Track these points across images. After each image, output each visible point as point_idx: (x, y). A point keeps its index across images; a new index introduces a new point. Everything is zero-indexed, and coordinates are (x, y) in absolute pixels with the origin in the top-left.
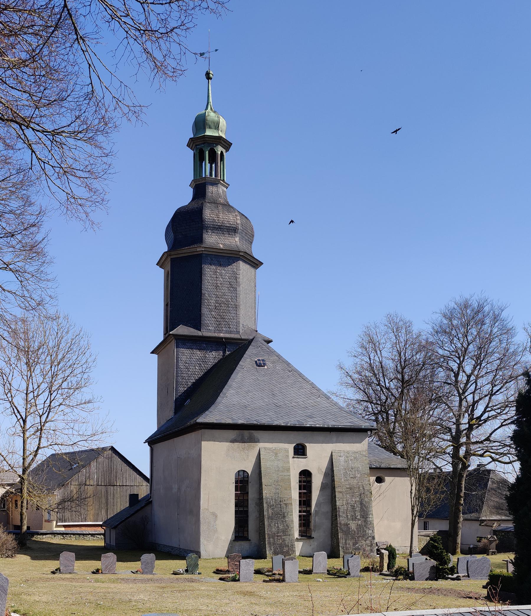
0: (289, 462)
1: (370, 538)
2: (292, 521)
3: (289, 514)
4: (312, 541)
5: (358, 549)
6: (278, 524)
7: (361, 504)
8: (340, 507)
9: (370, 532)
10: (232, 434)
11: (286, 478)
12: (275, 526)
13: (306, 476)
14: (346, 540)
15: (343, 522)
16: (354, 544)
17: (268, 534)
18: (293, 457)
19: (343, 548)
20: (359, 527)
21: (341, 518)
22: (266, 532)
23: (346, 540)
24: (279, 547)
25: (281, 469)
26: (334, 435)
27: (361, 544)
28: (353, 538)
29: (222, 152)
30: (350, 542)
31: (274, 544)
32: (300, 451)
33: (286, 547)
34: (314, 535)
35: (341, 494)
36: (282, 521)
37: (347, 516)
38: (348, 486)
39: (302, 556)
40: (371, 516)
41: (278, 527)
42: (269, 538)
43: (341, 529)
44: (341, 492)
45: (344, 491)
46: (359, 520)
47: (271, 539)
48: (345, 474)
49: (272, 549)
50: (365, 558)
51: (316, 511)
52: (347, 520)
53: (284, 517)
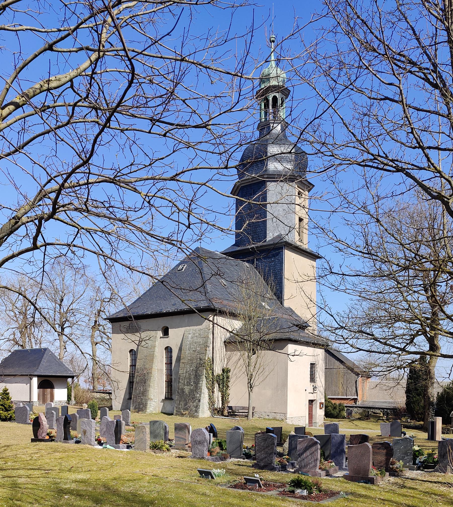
0: (155, 341)
1: (197, 401)
4: (172, 401)
7: (196, 372)
9: (198, 395)
10: (126, 324)
11: (152, 353)
13: (168, 350)
15: (180, 387)
16: (186, 404)
18: (161, 338)
19: (177, 407)
20: (191, 391)
21: (180, 384)
25: (150, 347)
26: (186, 318)
27: (189, 405)
28: (185, 400)
29: (275, 99)
32: (166, 332)
34: (173, 397)
35: (183, 365)
36: (144, 386)
37: (184, 382)
38: (189, 358)
39: (165, 413)
43: (178, 392)
44: (183, 363)
45: (186, 362)
46: (192, 385)
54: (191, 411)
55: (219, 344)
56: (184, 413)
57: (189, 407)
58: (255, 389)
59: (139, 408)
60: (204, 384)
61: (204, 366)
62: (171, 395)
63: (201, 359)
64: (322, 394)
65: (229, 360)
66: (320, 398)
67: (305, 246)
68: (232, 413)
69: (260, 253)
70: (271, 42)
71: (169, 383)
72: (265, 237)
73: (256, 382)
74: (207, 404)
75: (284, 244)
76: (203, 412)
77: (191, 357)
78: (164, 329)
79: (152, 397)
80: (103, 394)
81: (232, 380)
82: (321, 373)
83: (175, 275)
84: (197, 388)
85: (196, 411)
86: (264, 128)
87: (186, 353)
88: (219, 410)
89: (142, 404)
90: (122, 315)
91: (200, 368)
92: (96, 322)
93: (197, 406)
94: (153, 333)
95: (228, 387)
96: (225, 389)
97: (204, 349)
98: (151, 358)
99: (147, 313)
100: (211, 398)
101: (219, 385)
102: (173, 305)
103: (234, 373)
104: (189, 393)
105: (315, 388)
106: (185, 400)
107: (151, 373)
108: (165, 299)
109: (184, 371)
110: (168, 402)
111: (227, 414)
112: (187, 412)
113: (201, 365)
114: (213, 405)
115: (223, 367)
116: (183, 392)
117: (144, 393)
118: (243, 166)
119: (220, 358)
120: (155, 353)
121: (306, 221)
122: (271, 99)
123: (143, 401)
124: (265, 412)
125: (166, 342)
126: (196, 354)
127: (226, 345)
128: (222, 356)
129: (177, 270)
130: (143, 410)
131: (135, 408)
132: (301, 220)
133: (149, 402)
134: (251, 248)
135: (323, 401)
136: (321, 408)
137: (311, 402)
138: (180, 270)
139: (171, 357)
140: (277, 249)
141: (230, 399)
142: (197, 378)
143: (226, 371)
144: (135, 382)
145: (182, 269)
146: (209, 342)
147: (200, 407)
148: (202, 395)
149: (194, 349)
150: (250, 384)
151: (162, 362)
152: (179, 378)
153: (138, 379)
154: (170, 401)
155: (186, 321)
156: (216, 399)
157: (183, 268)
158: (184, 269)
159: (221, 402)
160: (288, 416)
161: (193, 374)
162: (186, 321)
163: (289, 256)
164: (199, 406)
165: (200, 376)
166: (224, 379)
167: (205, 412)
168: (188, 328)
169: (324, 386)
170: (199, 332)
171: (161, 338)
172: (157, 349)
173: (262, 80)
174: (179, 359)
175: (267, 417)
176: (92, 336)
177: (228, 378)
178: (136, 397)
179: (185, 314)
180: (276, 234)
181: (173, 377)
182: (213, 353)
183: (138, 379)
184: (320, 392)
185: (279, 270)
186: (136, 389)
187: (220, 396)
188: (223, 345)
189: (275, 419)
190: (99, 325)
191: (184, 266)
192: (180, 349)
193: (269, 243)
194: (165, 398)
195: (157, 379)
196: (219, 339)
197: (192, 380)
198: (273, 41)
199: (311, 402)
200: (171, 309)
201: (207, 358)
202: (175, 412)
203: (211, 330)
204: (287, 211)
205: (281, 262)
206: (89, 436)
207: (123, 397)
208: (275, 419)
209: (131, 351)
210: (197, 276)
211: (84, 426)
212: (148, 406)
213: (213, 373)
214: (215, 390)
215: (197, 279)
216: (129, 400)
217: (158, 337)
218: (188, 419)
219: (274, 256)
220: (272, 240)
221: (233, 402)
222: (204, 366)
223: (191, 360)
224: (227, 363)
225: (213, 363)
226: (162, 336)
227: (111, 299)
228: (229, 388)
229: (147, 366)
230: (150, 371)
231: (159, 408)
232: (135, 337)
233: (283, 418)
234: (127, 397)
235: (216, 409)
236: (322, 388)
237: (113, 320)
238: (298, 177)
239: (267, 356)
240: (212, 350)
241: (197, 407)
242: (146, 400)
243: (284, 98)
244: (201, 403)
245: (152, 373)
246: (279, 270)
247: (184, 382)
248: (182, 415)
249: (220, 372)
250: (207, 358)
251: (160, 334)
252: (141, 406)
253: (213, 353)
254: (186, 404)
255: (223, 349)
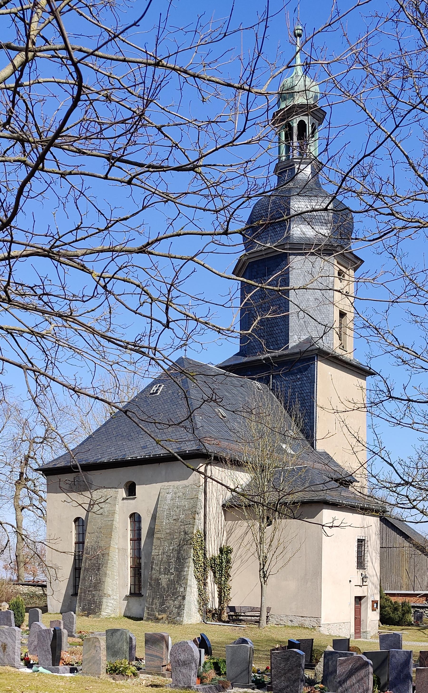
1: (180, 598)
2: (106, 574)
3: (104, 566)
4: (142, 598)
5: (163, 611)
6: (92, 577)
7: (179, 553)
8: (155, 557)
9: (182, 589)
10: (70, 477)
11: (110, 523)
12: (89, 579)
14: (153, 599)
16: (162, 603)
17: (81, 588)
18: (123, 499)
19: (148, 608)
20: (171, 583)
22: (80, 586)
23: (153, 599)
24: (88, 603)
27: (168, 604)
28: (161, 597)
29: (302, 125)
30: (157, 602)
31: (84, 599)
32: (131, 490)
33: (94, 604)
34: (143, 592)
36: (97, 574)
37: (160, 568)
38: (168, 531)
39: (129, 618)
40: (186, 569)
41: (91, 581)
42: (81, 593)
43: (151, 585)
44: (158, 539)
45: (163, 537)
47: (83, 594)
48: (169, 516)
49: (82, 605)
50: (169, 623)
51: (145, 562)
52: (160, 572)
53: (99, 569)
54: (170, 614)
55: (214, 509)
56: (160, 617)
57: (168, 608)
58: (271, 580)
59: (89, 609)
60: (191, 572)
61: (191, 544)
62: (140, 589)
63: (186, 533)
64: (376, 588)
65: (230, 533)
66: (372, 593)
67: (349, 356)
68: (235, 617)
69: (279, 366)
70: (296, 37)
71: (137, 570)
72: (287, 341)
73: (272, 568)
74: (196, 603)
75: (316, 352)
76: (190, 615)
77: (170, 529)
78: (128, 485)
79: (110, 592)
80: (34, 588)
81: (234, 566)
82: (374, 554)
83: (146, 401)
84: (180, 578)
85: (179, 614)
86: (285, 170)
87: (164, 523)
88: (214, 612)
89: (95, 603)
90: (62, 464)
91: (185, 547)
92: (21, 474)
93: (180, 606)
94: (110, 492)
95: (229, 576)
96: (223, 579)
97: (191, 517)
98: (108, 531)
99: (102, 460)
100: (201, 593)
101: (214, 573)
102: (143, 448)
103: (238, 555)
104: (167, 585)
105: (364, 578)
106: (161, 597)
107: (108, 554)
108: (130, 438)
109: (160, 550)
110: (134, 600)
111: (227, 619)
112: (164, 616)
113: (187, 542)
114: (206, 604)
115: (221, 545)
116: (159, 584)
117: (98, 586)
118: (252, 231)
119: (217, 530)
120: (114, 523)
121: (350, 316)
122: (295, 125)
123: (96, 598)
124: (287, 616)
125: (132, 506)
126: (178, 524)
127: (225, 511)
128: (220, 528)
129: (148, 393)
130: (95, 613)
131: (83, 610)
132: (342, 315)
133: (104, 600)
134: (265, 359)
135: (377, 598)
136: (373, 610)
137: (359, 599)
138: (153, 394)
139: (140, 529)
140: (306, 359)
141: (231, 596)
142: (181, 562)
143: (225, 551)
144: (83, 569)
145: (156, 392)
146: (199, 506)
147: (185, 608)
148: (188, 589)
149: (175, 517)
150: (263, 572)
151: (125, 537)
152: (153, 563)
153: (87, 564)
154: (137, 598)
155: (163, 473)
156: (210, 595)
157: (157, 390)
158: (159, 392)
159: (217, 600)
160: (323, 621)
161: (174, 556)
162: (163, 473)
163: (323, 371)
164: (184, 605)
165: (184, 559)
166: (222, 563)
167: (192, 616)
168: (166, 484)
169: (379, 574)
170: (182, 490)
171: (123, 499)
172: (117, 517)
173: (282, 97)
174: (151, 532)
175: (290, 624)
176: (16, 497)
177: (228, 561)
178: (85, 593)
179: (162, 462)
180: (304, 337)
181: (143, 561)
182: (205, 523)
183: (87, 564)
184: (373, 584)
185: (309, 394)
186: (84, 579)
187: (216, 590)
188: (220, 510)
189: (302, 626)
190: (27, 480)
191: (160, 386)
192: (154, 517)
193: (292, 351)
194: (131, 593)
195: (117, 563)
196: (214, 501)
197: (173, 566)
198: (300, 35)
199: (359, 599)
200: (139, 455)
201: (195, 532)
202: (145, 615)
203: (202, 488)
204: (320, 300)
205: (312, 381)
206: (11, 653)
207: (64, 592)
208: (302, 626)
209: (77, 520)
210: (180, 402)
211: (4, 637)
212: (104, 607)
213: (205, 554)
214: (208, 580)
215: (179, 407)
216: (74, 598)
217: (120, 498)
218: (166, 626)
219: (301, 372)
220: (297, 346)
221: (236, 600)
222: (191, 544)
223: (170, 534)
224: (227, 540)
225: (205, 539)
226: (125, 496)
227: (45, 438)
228: (230, 578)
229: (102, 544)
230: (106, 551)
231: (120, 609)
232: (84, 498)
233: (315, 625)
234: (71, 592)
235: (210, 611)
236: (375, 577)
237: (48, 471)
238: (339, 248)
239: (289, 528)
240: (203, 518)
241: (180, 607)
242: (101, 597)
243: (317, 125)
244: (186, 602)
245: (110, 554)
246: (309, 394)
247: (160, 568)
248: (157, 620)
249: (217, 553)
250: (195, 532)
251: (122, 493)
252: (93, 606)
253: (205, 523)
254: (162, 603)
255: (220, 516)
